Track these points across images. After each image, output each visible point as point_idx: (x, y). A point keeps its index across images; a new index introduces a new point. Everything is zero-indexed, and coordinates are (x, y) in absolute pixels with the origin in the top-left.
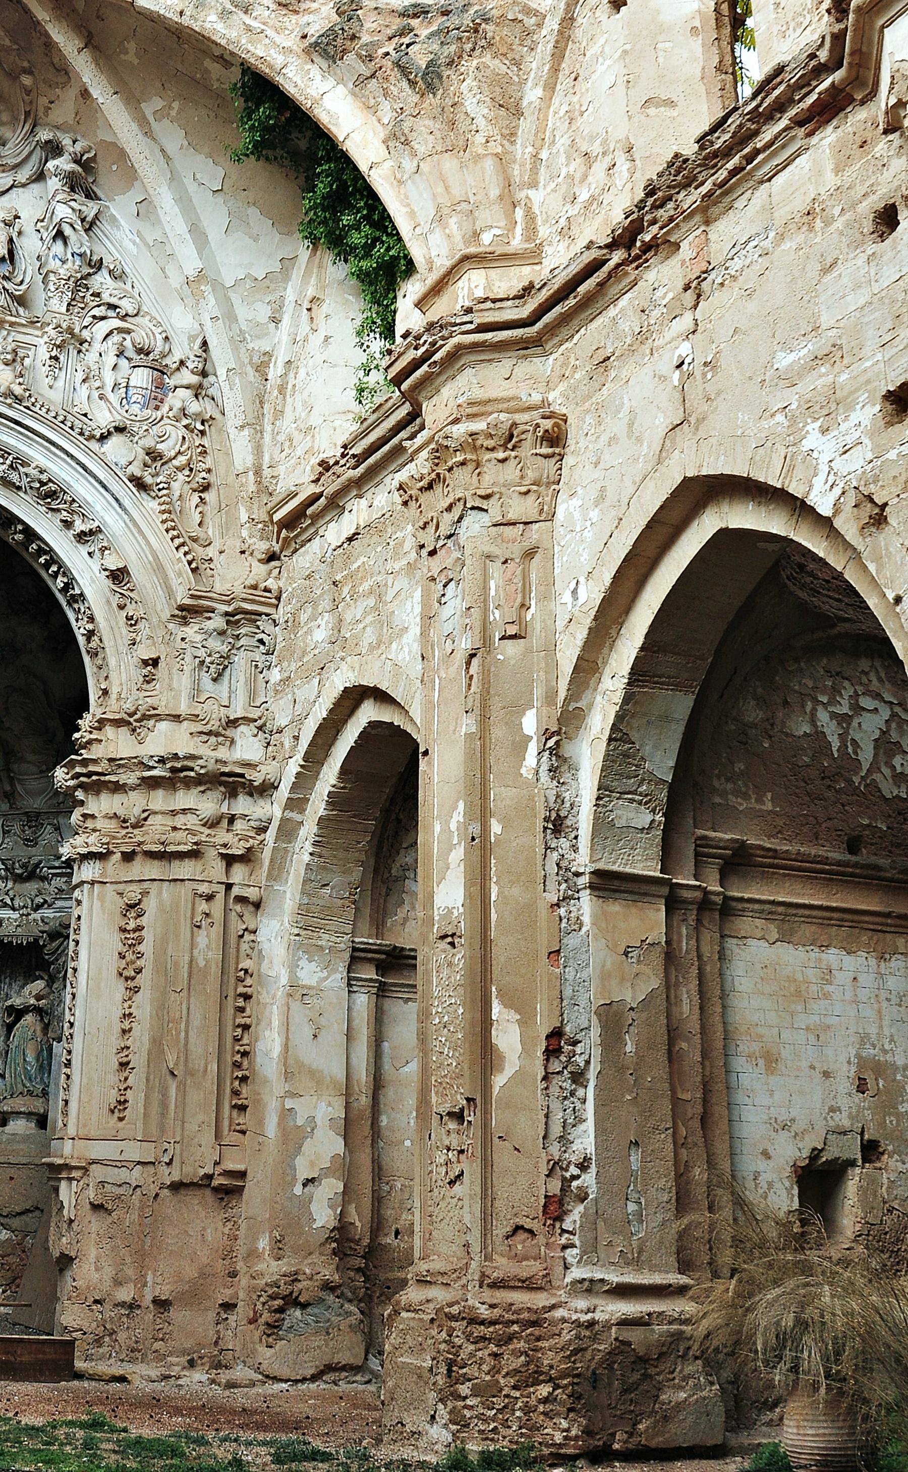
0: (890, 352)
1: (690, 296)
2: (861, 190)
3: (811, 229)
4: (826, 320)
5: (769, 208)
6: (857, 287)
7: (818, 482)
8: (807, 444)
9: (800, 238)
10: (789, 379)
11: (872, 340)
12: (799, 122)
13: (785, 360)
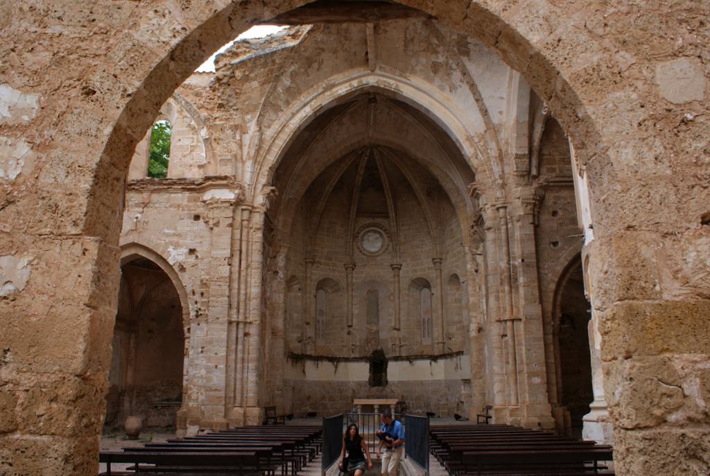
0: (193, 242)
1: (142, 205)
2: (192, 208)
3: (179, 209)
4: (178, 228)
5: (169, 200)
6: (188, 226)
7: (170, 258)
8: (169, 250)
9: (176, 209)
10: (168, 235)
11: (189, 238)
12: (183, 188)
13: (167, 231)
